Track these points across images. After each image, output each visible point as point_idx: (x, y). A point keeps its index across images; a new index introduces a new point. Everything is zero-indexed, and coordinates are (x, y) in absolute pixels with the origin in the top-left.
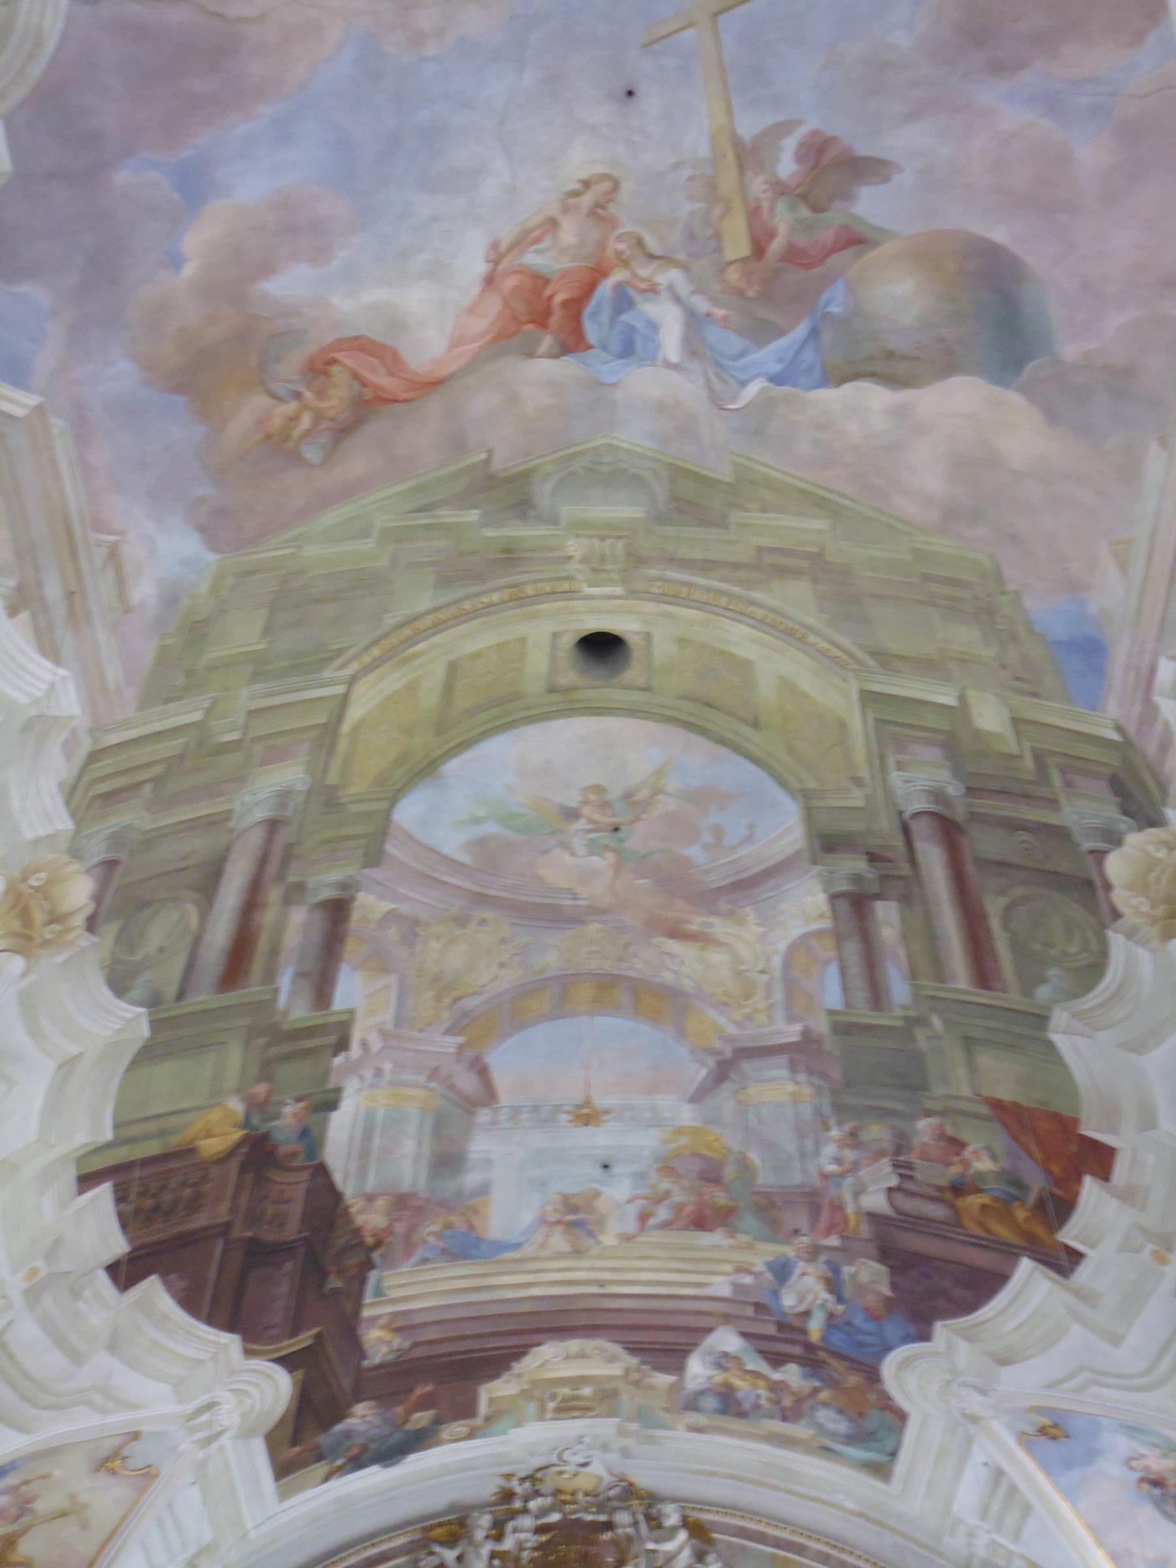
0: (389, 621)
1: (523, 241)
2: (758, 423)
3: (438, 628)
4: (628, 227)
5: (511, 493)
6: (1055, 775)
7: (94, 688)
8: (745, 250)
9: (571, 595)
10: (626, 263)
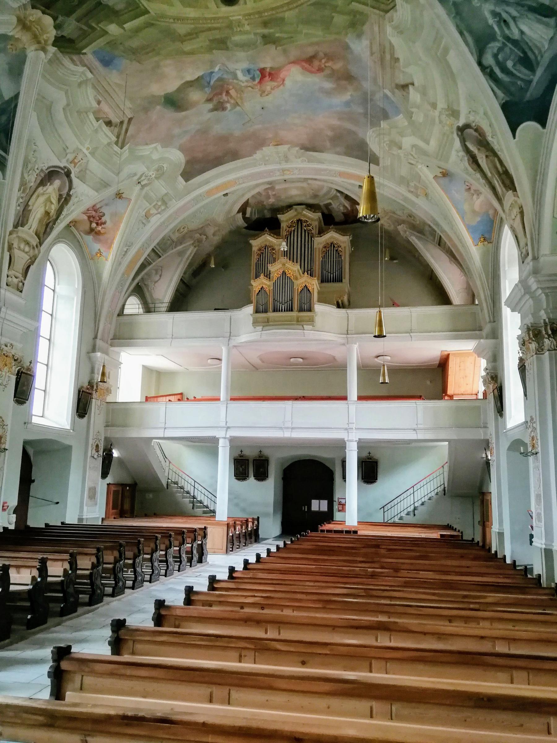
0: (297, 10)
1: (278, 86)
2: (212, 64)
3: (282, 6)
5: (268, 40)
6: (85, 28)
7: (382, 30)
9: (245, 15)
10: (254, 85)
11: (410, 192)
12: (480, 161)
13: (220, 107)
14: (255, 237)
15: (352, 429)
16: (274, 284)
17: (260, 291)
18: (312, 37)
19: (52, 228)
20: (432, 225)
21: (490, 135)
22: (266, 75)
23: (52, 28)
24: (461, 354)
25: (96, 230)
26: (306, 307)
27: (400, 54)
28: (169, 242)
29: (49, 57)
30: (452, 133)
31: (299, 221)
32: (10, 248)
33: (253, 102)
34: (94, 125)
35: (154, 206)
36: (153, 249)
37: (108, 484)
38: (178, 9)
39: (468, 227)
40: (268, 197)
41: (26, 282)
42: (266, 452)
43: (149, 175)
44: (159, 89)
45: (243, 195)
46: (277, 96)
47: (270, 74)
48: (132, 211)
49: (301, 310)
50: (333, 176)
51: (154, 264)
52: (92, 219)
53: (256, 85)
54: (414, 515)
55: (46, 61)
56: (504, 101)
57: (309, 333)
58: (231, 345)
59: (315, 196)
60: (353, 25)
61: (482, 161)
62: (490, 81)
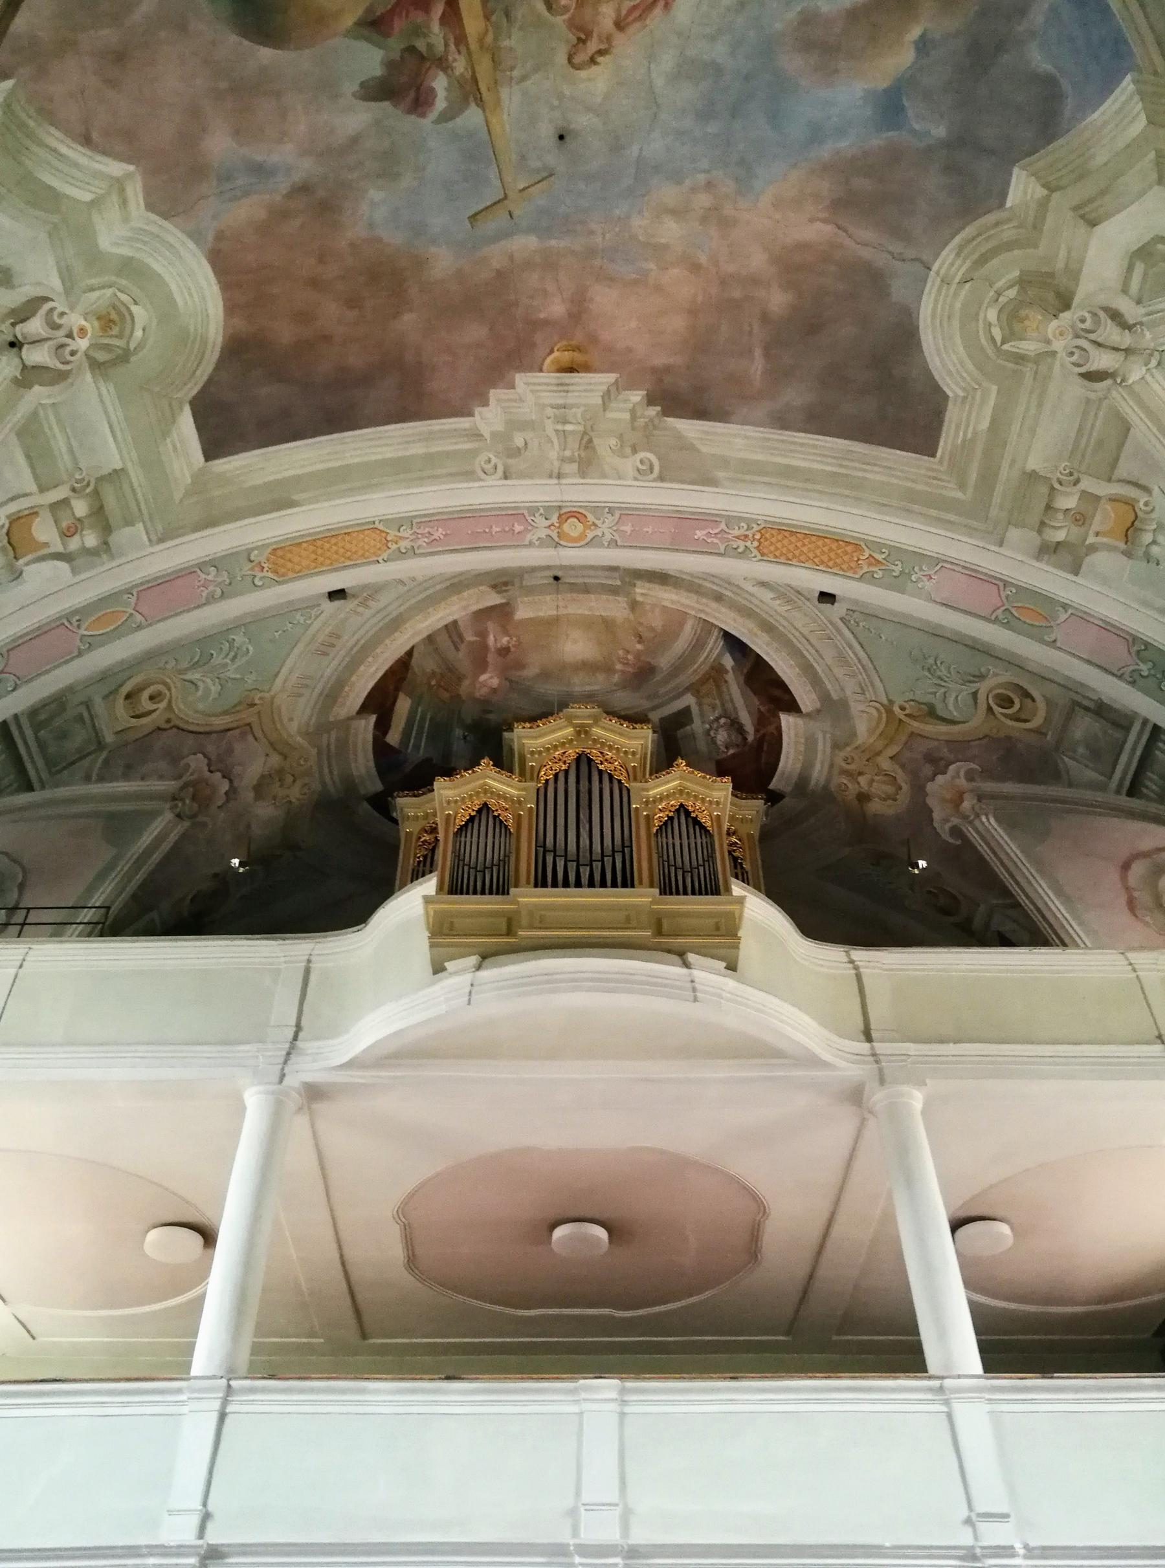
4: (560, 20)
16: (541, 795)
17: (472, 818)
28: (80, 736)
35: (55, 507)
45: (395, 624)
58: (293, 1080)
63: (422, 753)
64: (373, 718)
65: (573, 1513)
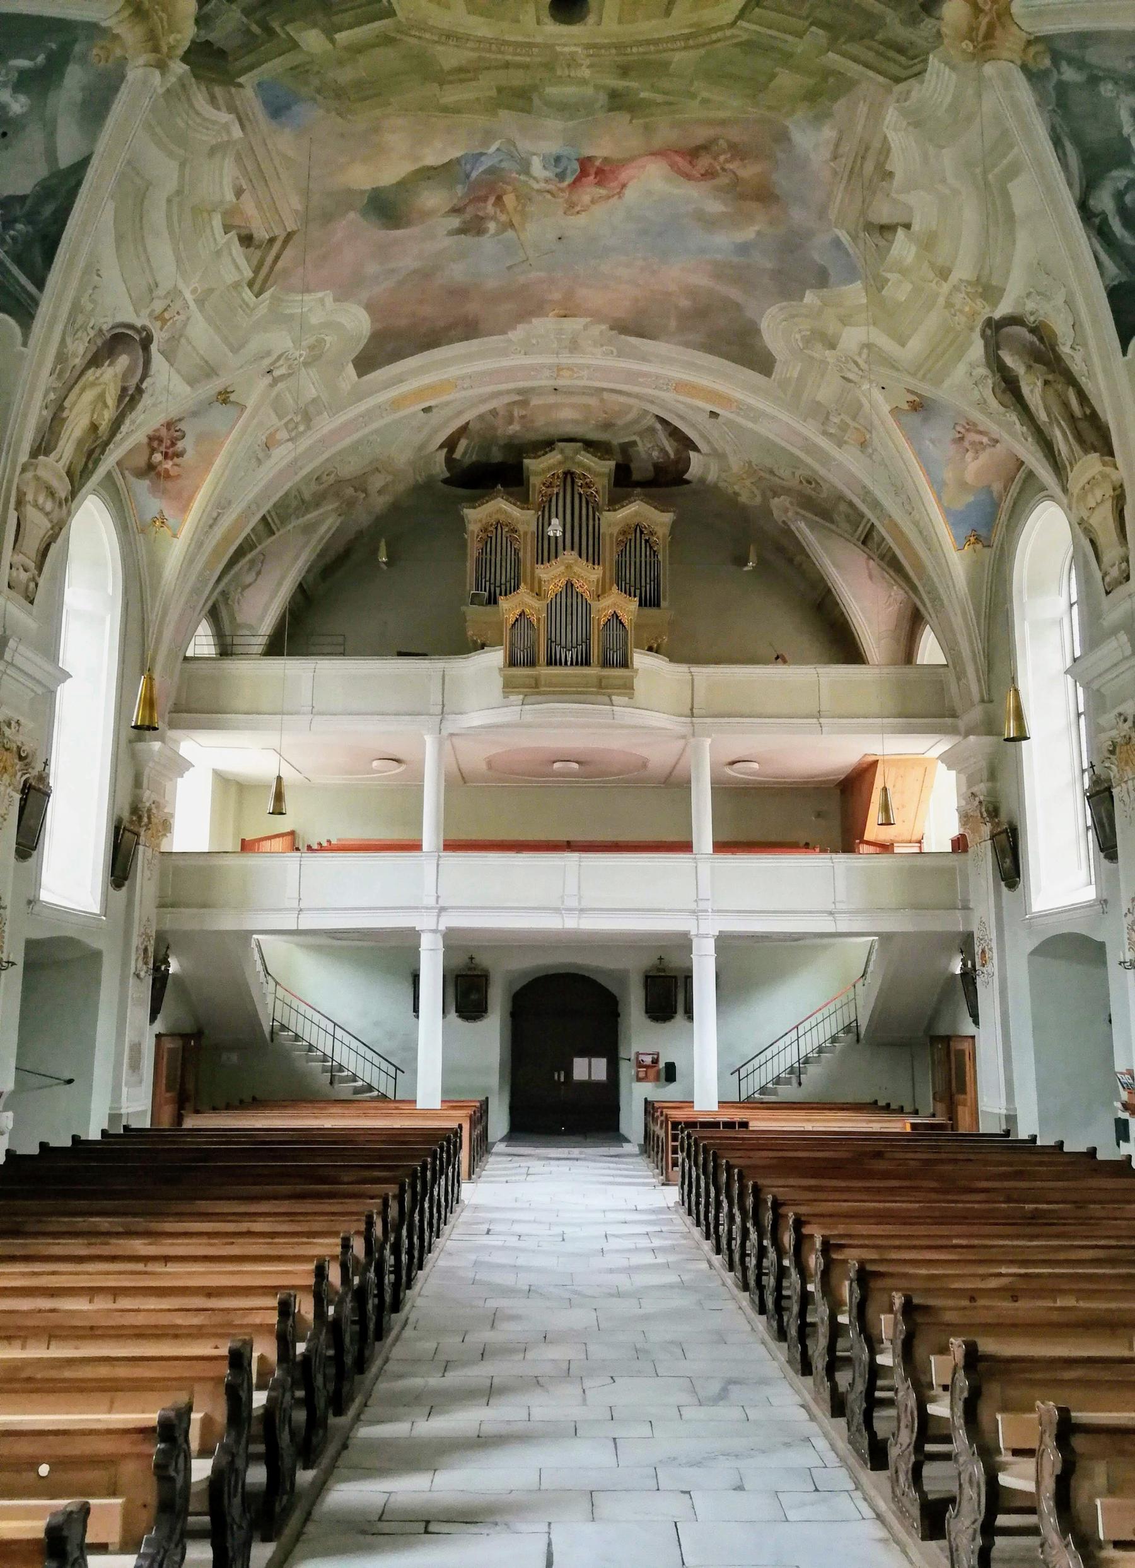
0: (702, 51)
2: (489, 136)
3: (674, 39)
4: (561, 200)
5: (618, 101)
6: (255, 29)
7: (876, 115)
8: (505, 198)
9: (587, 47)
11: (825, 433)
12: (1025, 390)
13: (474, 227)
14: (474, 502)
15: (707, 911)
16: (549, 607)
17: (517, 620)
18: (722, 108)
19: (97, 462)
20: (857, 501)
21: (1069, 343)
22: (592, 172)
23: (192, 22)
24: (902, 762)
25: (159, 468)
26: (616, 657)
27: (896, 164)
28: (294, 503)
29: (169, 85)
30: (972, 329)
31: (569, 475)
32: (19, 504)
33: (540, 228)
34: (217, 236)
36: (264, 518)
37: (157, 1036)
38: (459, 18)
39: (948, 513)
40: (510, 420)
41: (41, 581)
42: (485, 960)
43: (294, 356)
44: (364, 176)
45: (460, 413)
46: (600, 216)
47: (600, 172)
48: (243, 432)
49: (606, 663)
50: (661, 389)
51: (259, 548)
52: (155, 444)
53: (562, 190)
54: (800, 1084)
55: (161, 91)
56: (1116, 283)
57: (623, 711)
58: (445, 733)
59: (607, 426)
60: (811, 96)
61: (1032, 391)
62: (1094, 240)
63: (474, 458)
64: (445, 450)
65: (562, 897)
